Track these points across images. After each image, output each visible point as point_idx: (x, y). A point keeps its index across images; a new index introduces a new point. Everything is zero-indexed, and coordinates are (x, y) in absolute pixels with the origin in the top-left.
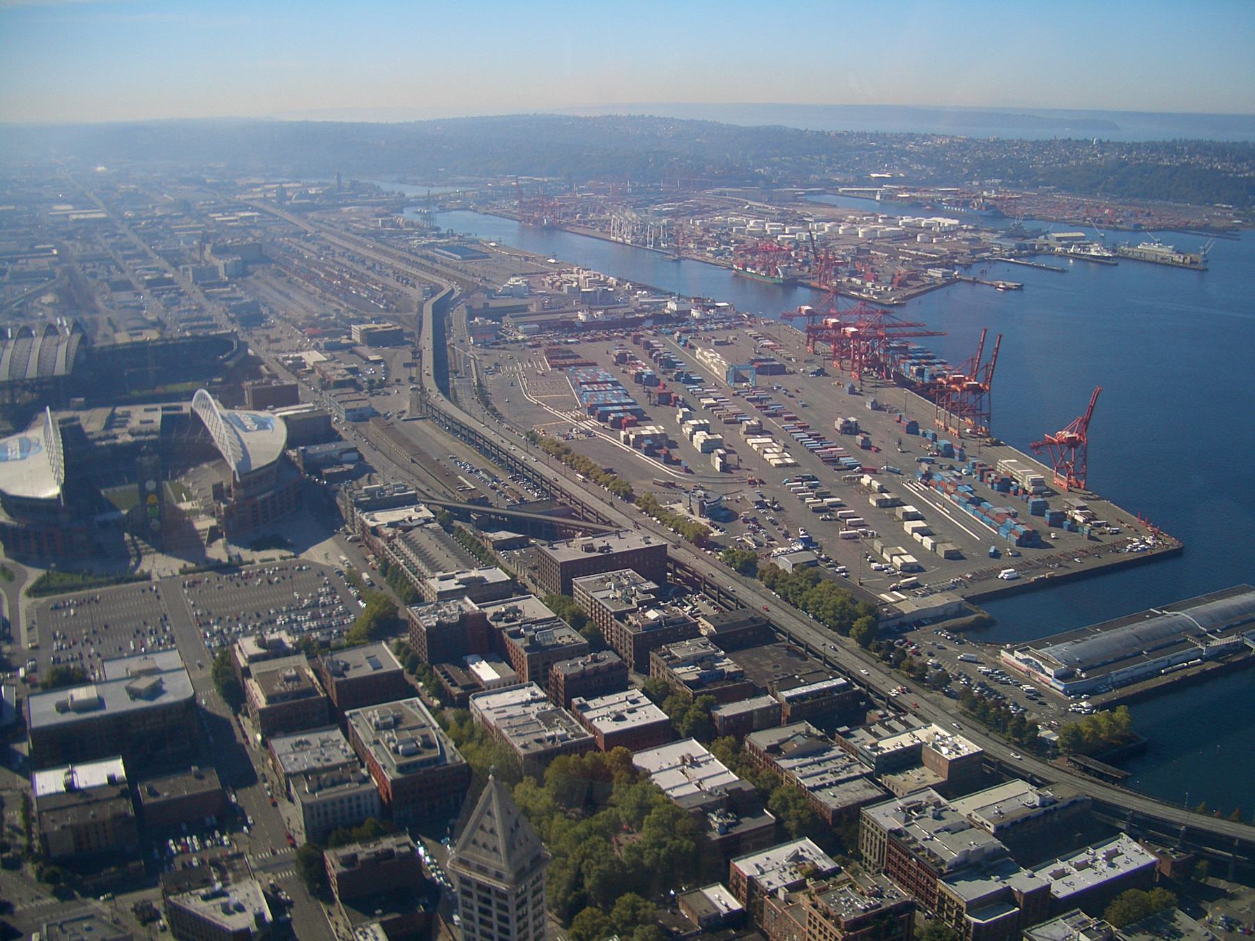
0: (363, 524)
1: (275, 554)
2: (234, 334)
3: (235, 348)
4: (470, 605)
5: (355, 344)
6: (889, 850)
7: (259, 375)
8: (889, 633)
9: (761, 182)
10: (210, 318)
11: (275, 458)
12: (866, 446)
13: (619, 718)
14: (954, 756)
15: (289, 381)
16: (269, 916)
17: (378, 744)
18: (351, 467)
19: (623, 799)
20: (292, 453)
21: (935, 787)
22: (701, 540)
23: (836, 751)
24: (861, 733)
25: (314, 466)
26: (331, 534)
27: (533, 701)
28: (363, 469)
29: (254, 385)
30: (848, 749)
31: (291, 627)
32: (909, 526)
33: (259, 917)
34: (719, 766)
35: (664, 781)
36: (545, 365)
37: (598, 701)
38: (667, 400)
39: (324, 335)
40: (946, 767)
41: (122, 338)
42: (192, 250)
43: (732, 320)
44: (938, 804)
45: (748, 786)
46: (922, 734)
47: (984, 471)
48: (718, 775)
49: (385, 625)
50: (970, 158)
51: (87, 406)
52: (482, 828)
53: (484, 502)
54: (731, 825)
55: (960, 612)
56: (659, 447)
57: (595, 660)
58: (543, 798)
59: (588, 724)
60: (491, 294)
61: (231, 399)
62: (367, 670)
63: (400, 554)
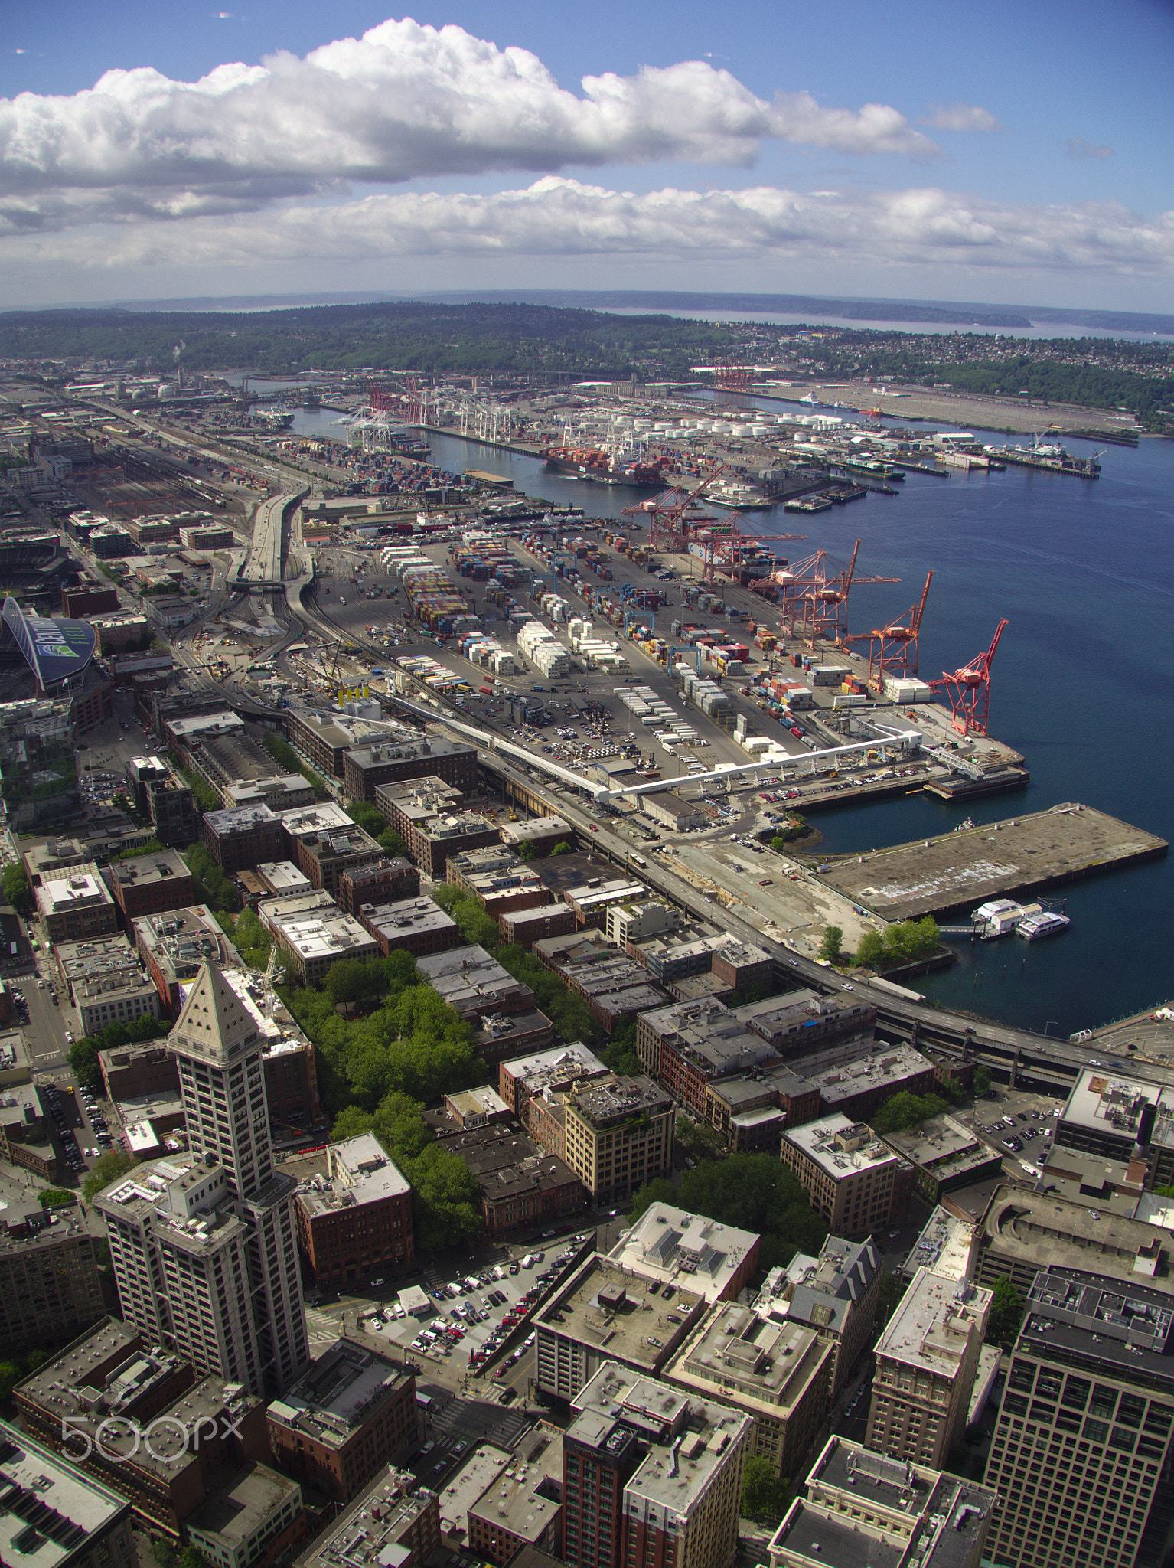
6: (664, 1056)
7: (76, 581)
9: (633, 376)
14: (742, 964)
16: (39, 1112)
21: (717, 996)
27: (322, 907)
33: (30, 1112)
34: (500, 971)
35: (441, 986)
37: (384, 909)
40: (734, 976)
42: (22, 452)
44: (715, 1009)
50: (862, 352)
52: (196, 1007)
54: (506, 1029)
57: (386, 865)
62: (156, 877)
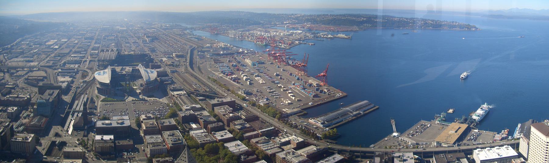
1: (152, 99)
4: (192, 112)
8: (284, 117)
12: (281, 78)
13: (222, 136)
17: (168, 139)
19: (222, 153)
22: (244, 99)
23: (271, 142)
24: (277, 138)
26: (165, 96)
28: (173, 83)
30: (274, 142)
31: (153, 114)
32: (289, 95)
35: (231, 149)
36: (213, 63)
37: (218, 133)
38: (238, 70)
41: (126, 53)
43: (253, 53)
45: (250, 150)
46: (291, 138)
47: (306, 82)
48: (244, 148)
49: (174, 115)
51: (118, 66)
53: (198, 91)
55: (300, 112)
56: (236, 80)
58: (203, 152)
59: (215, 137)
60: (203, 47)
62: (168, 124)
63: (178, 101)
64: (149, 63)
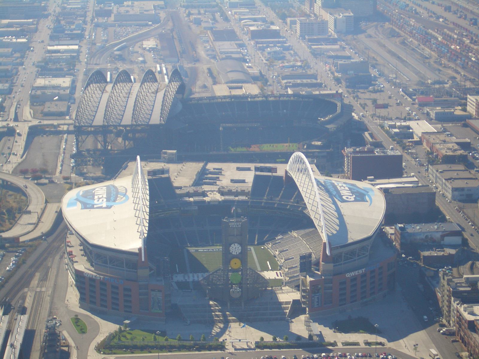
0: (460, 317)
1: (360, 338)
2: (339, 96)
3: (339, 110)
5: (470, 117)
7: (362, 142)
10: (315, 77)
11: (370, 234)
15: (393, 150)
18: (453, 252)
20: (389, 230)
25: (411, 246)
26: (424, 326)
29: (355, 152)
39: (437, 104)
41: (221, 90)
51: (180, 159)
61: (329, 164)
64: (347, 148)
